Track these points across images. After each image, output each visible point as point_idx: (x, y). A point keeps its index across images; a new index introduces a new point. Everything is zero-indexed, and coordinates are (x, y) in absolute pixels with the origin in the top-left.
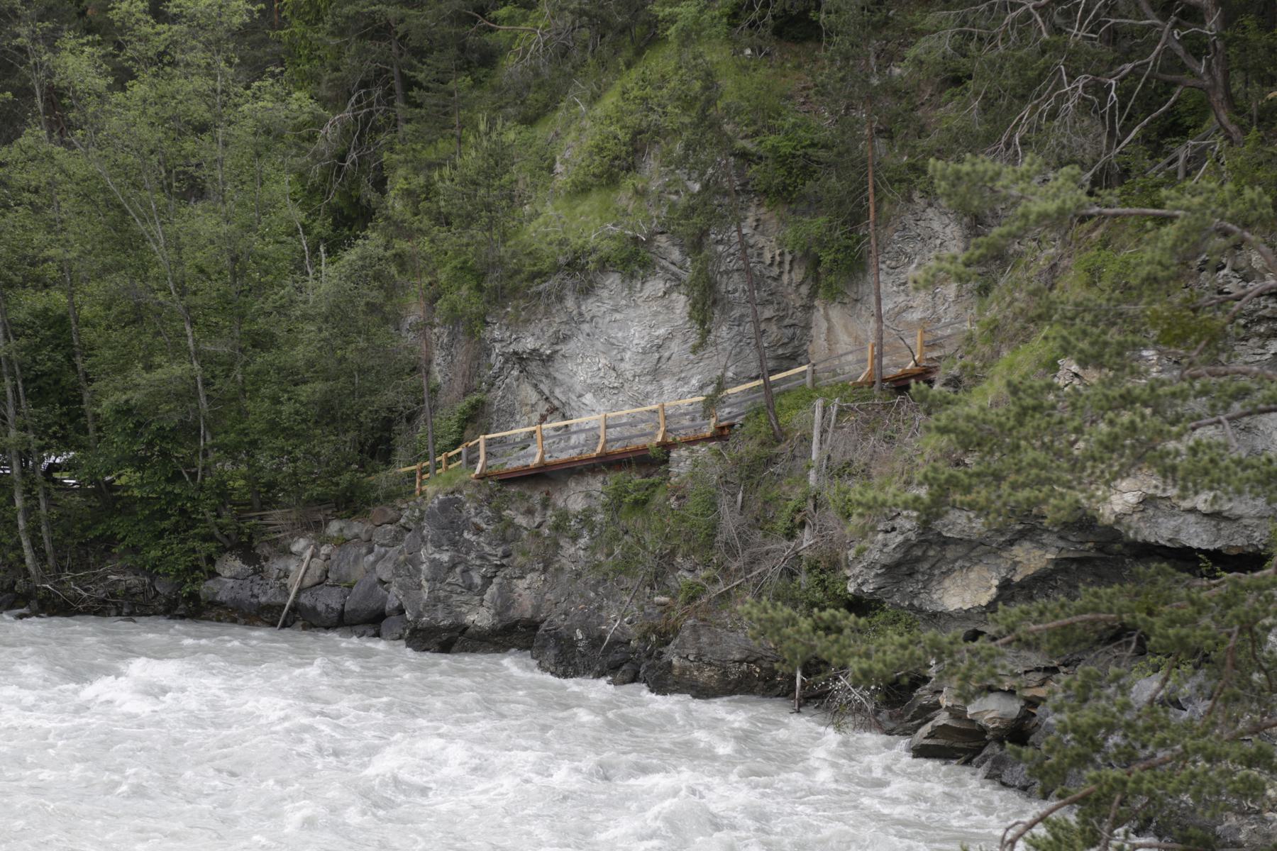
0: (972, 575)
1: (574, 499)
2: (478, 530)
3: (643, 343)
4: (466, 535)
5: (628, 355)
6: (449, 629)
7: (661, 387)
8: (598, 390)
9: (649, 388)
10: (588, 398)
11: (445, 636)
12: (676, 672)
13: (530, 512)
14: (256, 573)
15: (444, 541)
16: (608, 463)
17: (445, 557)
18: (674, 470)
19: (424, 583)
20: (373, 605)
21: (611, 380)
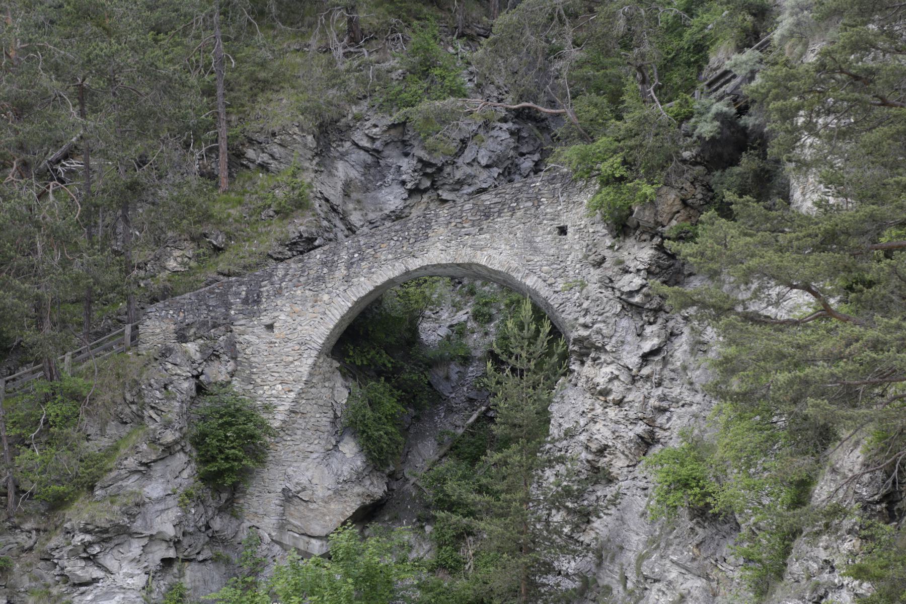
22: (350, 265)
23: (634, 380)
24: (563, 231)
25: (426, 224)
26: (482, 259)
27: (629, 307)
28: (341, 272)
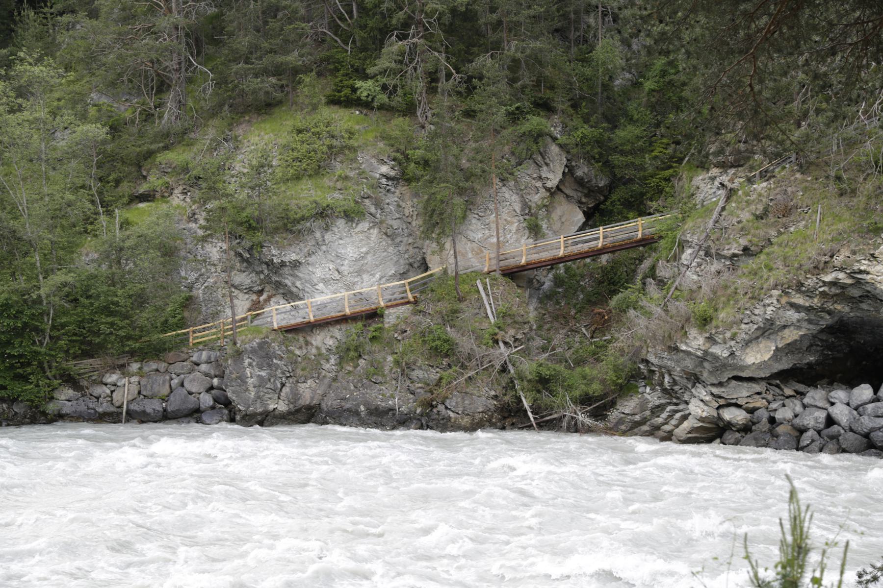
0: (761, 345)
1: (324, 340)
2: (281, 358)
3: (355, 256)
4: (275, 361)
5: (346, 262)
6: (261, 414)
7: (362, 279)
8: (325, 281)
9: (356, 279)
10: (321, 286)
11: (259, 418)
12: (453, 420)
13: (301, 348)
14: (83, 396)
15: (265, 365)
16: (343, 320)
17: (263, 374)
18: (386, 320)
19: (251, 388)
20: (191, 406)
21: (336, 276)
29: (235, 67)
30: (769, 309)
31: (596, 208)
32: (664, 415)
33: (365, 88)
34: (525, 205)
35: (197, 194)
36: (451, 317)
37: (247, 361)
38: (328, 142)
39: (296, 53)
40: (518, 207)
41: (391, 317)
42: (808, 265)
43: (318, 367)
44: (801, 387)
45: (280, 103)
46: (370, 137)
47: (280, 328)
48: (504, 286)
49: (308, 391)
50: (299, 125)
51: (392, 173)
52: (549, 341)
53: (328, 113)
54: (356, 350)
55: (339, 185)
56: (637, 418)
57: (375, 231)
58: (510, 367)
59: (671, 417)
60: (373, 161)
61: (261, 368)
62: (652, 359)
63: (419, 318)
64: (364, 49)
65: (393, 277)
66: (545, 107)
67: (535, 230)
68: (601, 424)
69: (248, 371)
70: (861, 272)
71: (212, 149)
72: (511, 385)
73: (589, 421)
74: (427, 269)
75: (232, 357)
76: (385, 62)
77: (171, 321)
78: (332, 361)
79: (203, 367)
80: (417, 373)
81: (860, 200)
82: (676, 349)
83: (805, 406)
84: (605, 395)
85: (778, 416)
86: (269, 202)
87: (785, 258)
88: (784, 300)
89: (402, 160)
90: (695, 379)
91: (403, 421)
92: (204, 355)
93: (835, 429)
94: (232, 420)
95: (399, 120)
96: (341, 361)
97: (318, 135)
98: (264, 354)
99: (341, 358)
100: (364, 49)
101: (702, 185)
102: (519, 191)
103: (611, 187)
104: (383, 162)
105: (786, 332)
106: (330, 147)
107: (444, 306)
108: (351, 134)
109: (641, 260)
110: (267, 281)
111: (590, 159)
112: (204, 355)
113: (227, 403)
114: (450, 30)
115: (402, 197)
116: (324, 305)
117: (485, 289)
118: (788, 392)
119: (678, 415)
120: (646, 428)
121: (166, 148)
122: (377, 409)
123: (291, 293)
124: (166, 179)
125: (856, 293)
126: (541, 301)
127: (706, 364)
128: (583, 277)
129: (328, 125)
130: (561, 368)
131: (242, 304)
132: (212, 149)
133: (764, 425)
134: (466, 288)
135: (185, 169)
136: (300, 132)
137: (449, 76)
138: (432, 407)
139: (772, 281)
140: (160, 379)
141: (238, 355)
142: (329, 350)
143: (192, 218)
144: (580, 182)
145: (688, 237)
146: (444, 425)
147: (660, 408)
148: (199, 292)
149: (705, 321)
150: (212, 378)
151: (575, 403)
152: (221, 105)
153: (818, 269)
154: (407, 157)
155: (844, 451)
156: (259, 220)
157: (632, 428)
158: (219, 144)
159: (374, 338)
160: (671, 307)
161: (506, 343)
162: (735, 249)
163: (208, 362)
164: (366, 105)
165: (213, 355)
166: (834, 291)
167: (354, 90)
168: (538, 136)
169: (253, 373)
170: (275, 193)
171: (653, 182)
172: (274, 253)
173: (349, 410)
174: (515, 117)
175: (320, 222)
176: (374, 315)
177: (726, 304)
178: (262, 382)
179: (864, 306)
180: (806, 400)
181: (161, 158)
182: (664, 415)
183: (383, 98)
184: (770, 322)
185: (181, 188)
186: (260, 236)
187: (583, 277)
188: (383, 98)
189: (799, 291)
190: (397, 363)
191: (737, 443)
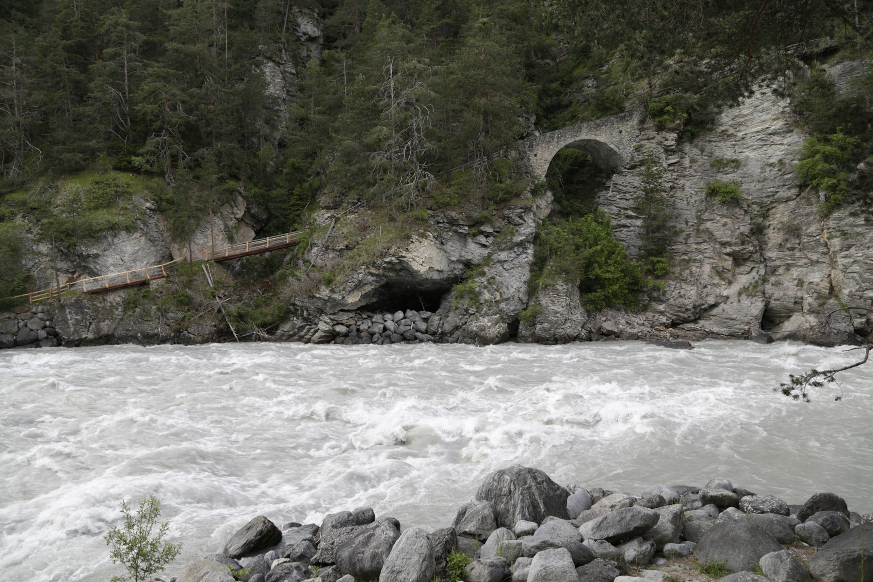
1: (115, 298)
2: (89, 309)
8: (114, 265)
10: (112, 268)
16: (126, 287)
17: (78, 317)
22: (558, 138)
23: (665, 171)
24: (621, 132)
25: (580, 128)
26: (598, 139)
27: (668, 151)
28: (556, 140)
29: (56, 148)
30: (361, 276)
31: (261, 229)
32: (305, 331)
33: (137, 161)
34: (226, 226)
35: (32, 218)
36: (189, 284)
37: (68, 311)
38: (115, 189)
39: (94, 141)
40: (222, 227)
41: (154, 285)
42: (378, 254)
43: (112, 313)
44: (370, 314)
45: (83, 169)
46: (139, 187)
47: (88, 292)
48: (216, 268)
49: (106, 327)
50: (97, 179)
51: (153, 207)
52: (241, 296)
53: (113, 174)
54: (134, 303)
55: (122, 212)
56: (291, 333)
57: (143, 238)
58: (223, 310)
59: (308, 331)
60: (142, 200)
61: (77, 314)
62: (298, 303)
63: (171, 285)
64: (134, 141)
65: (153, 264)
66: (236, 178)
67: (231, 239)
68: (273, 337)
69: (69, 317)
70: (402, 257)
71: (41, 193)
72: (223, 319)
73: (266, 336)
74: (172, 259)
75: (58, 308)
76: (149, 146)
77: (17, 289)
78: (120, 310)
79: (40, 315)
80: (170, 315)
81: (399, 224)
82: (314, 297)
83: (372, 323)
84: (274, 322)
85: (361, 328)
86: (80, 221)
87: (367, 251)
88: (367, 271)
89: (158, 200)
90: (321, 311)
91: (163, 341)
92: (40, 308)
93: (388, 332)
94: (59, 345)
95: (156, 179)
96: (125, 310)
97: (109, 185)
98: (78, 306)
99: (125, 308)
100: (134, 141)
101: (317, 218)
102: (223, 218)
103: (268, 220)
104: (147, 201)
105: (366, 287)
106: (116, 192)
107: (184, 278)
108: (129, 185)
109: (285, 255)
110: (79, 266)
111: (259, 204)
112: (40, 308)
113: (56, 335)
114: (184, 136)
115: (158, 220)
116: (113, 279)
117: (207, 269)
118: (364, 316)
119: (312, 330)
120: (296, 337)
121: (11, 192)
122: (148, 334)
123: (94, 272)
124: (12, 209)
125: (398, 267)
126: (234, 276)
127: (328, 304)
128: (256, 264)
129: (114, 180)
130: (249, 309)
131: (63, 280)
132: (41, 193)
133: (354, 333)
134: (196, 268)
135: (24, 203)
136: (97, 183)
137: (184, 158)
138: (180, 332)
139: (361, 261)
140: (12, 323)
141: (62, 307)
142: (118, 304)
143: (29, 231)
144: (253, 216)
145: (316, 241)
146: (188, 341)
147: (303, 327)
148: (35, 273)
149: (329, 282)
150: (45, 321)
151: (258, 327)
152: (46, 170)
153: (383, 255)
154: (161, 199)
155: (393, 342)
156: (73, 230)
157: (289, 338)
158: (46, 190)
159: (144, 296)
160: (312, 275)
161: (219, 297)
162: (342, 246)
163: (43, 312)
164: (136, 171)
165: (45, 308)
166: (390, 266)
167: (130, 162)
168: (232, 191)
169: (71, 317)
170: (83, 216)
171: (291, 217)
172: (83, 249)
173: (131, 336)
174: (221, 180)
175: (111, 232)
176: (144, 284)
177: (339, 273)
178: (77, 322)
179: (402, 274)
180: (373, 320)
181: (7, 197)
182: (305, 331)
183: (148, 167)
184: (360, 281)
185: (21, 214)
186: (74, 239)
187: (256, 264)
188: (148, 167)
189: (373, 266)
190: (159, 309)
191: (342, 343)
